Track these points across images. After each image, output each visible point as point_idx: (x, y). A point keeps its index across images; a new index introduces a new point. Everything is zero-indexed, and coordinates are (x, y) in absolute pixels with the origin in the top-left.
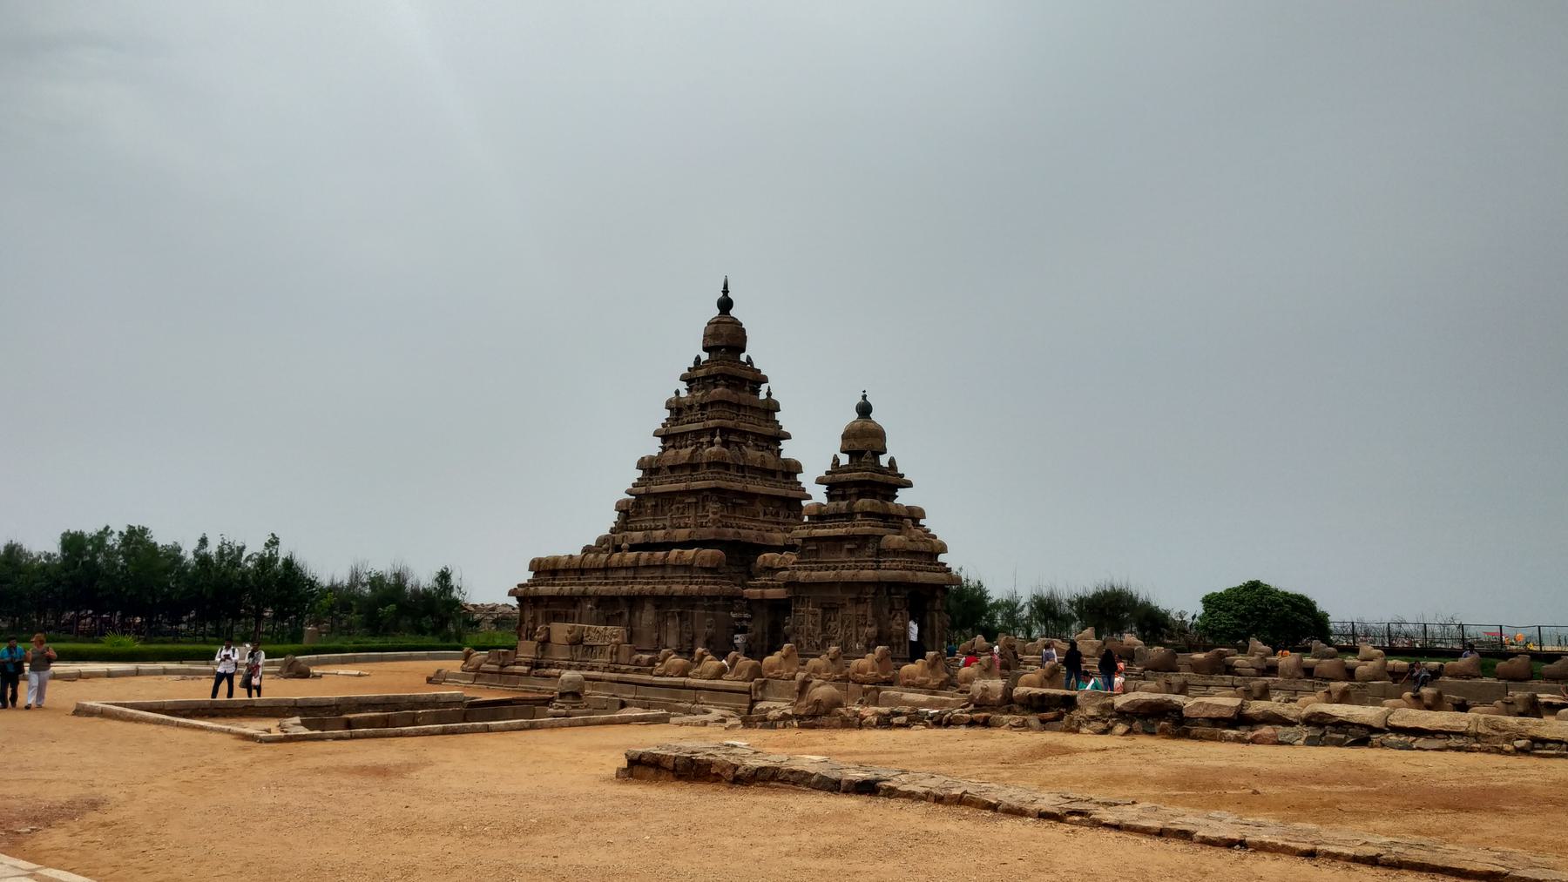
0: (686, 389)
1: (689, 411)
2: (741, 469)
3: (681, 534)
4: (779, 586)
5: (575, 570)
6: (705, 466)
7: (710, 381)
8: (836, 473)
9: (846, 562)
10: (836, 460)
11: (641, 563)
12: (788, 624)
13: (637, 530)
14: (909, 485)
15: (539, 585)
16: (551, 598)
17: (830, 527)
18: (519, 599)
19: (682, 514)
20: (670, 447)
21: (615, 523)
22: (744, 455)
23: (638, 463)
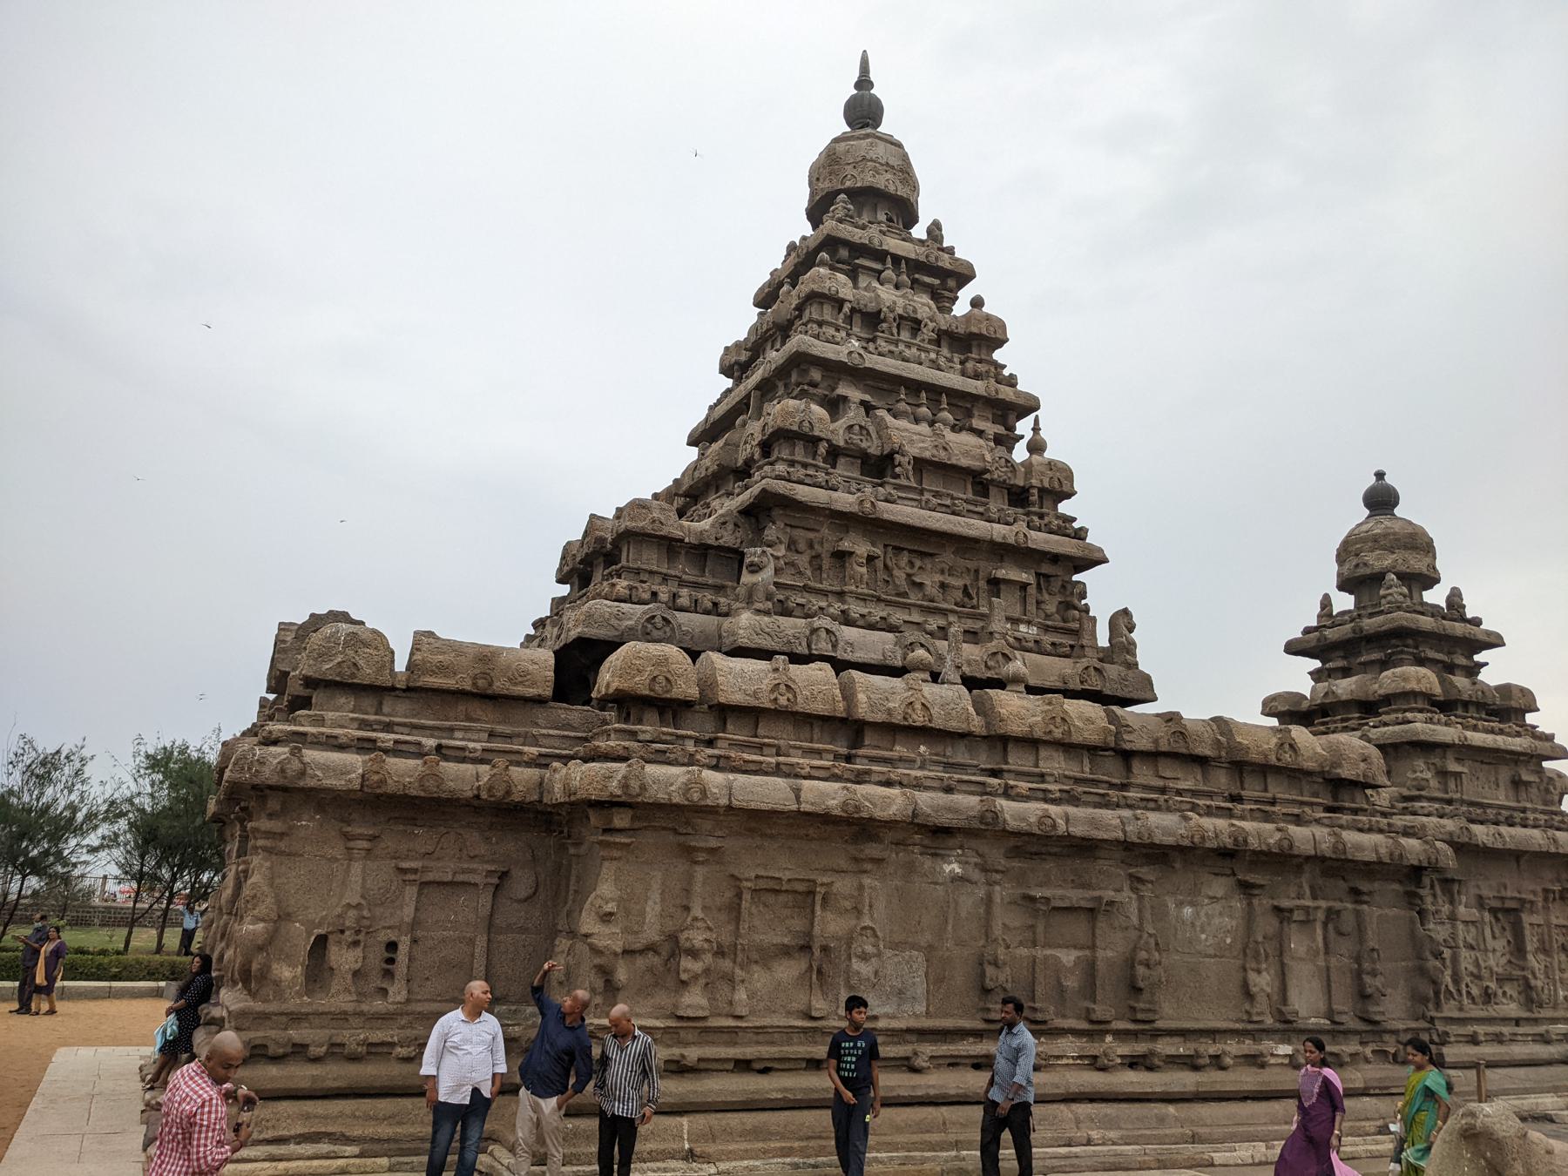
6: (1035, 498)
9: (1524, 810)
17: (1492, 731)
19: (956, 604)
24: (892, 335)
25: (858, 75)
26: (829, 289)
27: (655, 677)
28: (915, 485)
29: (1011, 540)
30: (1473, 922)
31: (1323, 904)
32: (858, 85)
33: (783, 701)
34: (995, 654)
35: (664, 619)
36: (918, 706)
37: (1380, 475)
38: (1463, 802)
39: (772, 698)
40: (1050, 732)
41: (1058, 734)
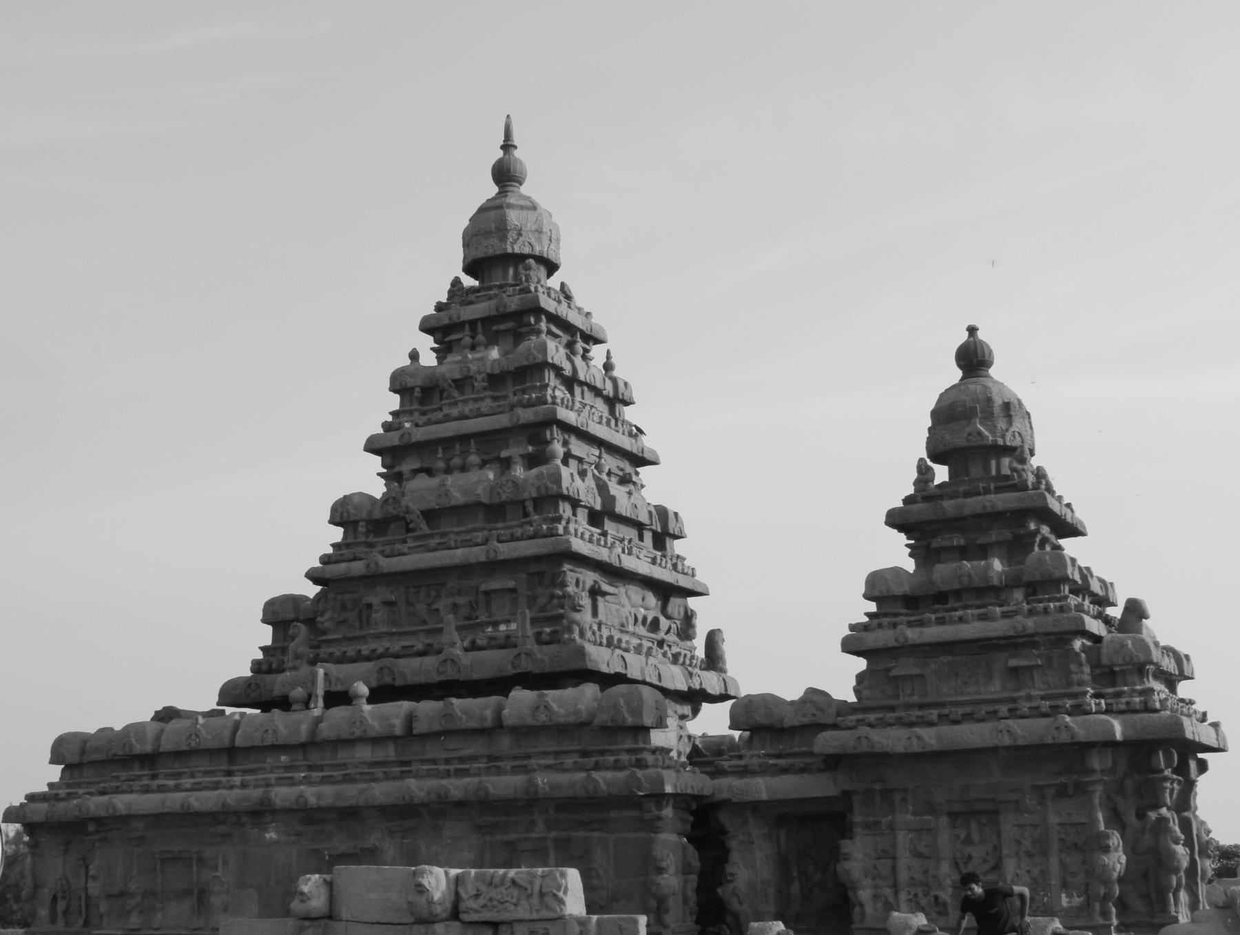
0: (432, 349)
1: (455, 393)
2: (595, 518)
3: (491, 662)
4: (802, 770)
5: (211, 753)
6: (530, 509)
7: (503, 327)
8: (941, 497)
9: (1014, 700)
10: (924, 473)
11: (419, 728)
12: (847, 857)
13: (343, 659)
14: (1073, 530)
15: (117, 791)
16: (158, 819)
17: (961, 620)
18: (30, 827)
19: (468, 618)
20: (416, 472)
21: (263, 649)
22: (602, 488)
23: (334, 509)
24: (454, 398)
25: (503, 138)
26: (401, 384)
27: (125, 744)
28: (428, 531)
29: (483, 559)
30: (929, 830)
31: (553, 834)
32: (503, 147)
33: (193, 744)
34: (445, 661)
35: (256, 684)
36: (270, 732)
37: (972, 330)
38: (909, 706)
39: (188, 742)
40: (354, 733)
41: (358, 733)
